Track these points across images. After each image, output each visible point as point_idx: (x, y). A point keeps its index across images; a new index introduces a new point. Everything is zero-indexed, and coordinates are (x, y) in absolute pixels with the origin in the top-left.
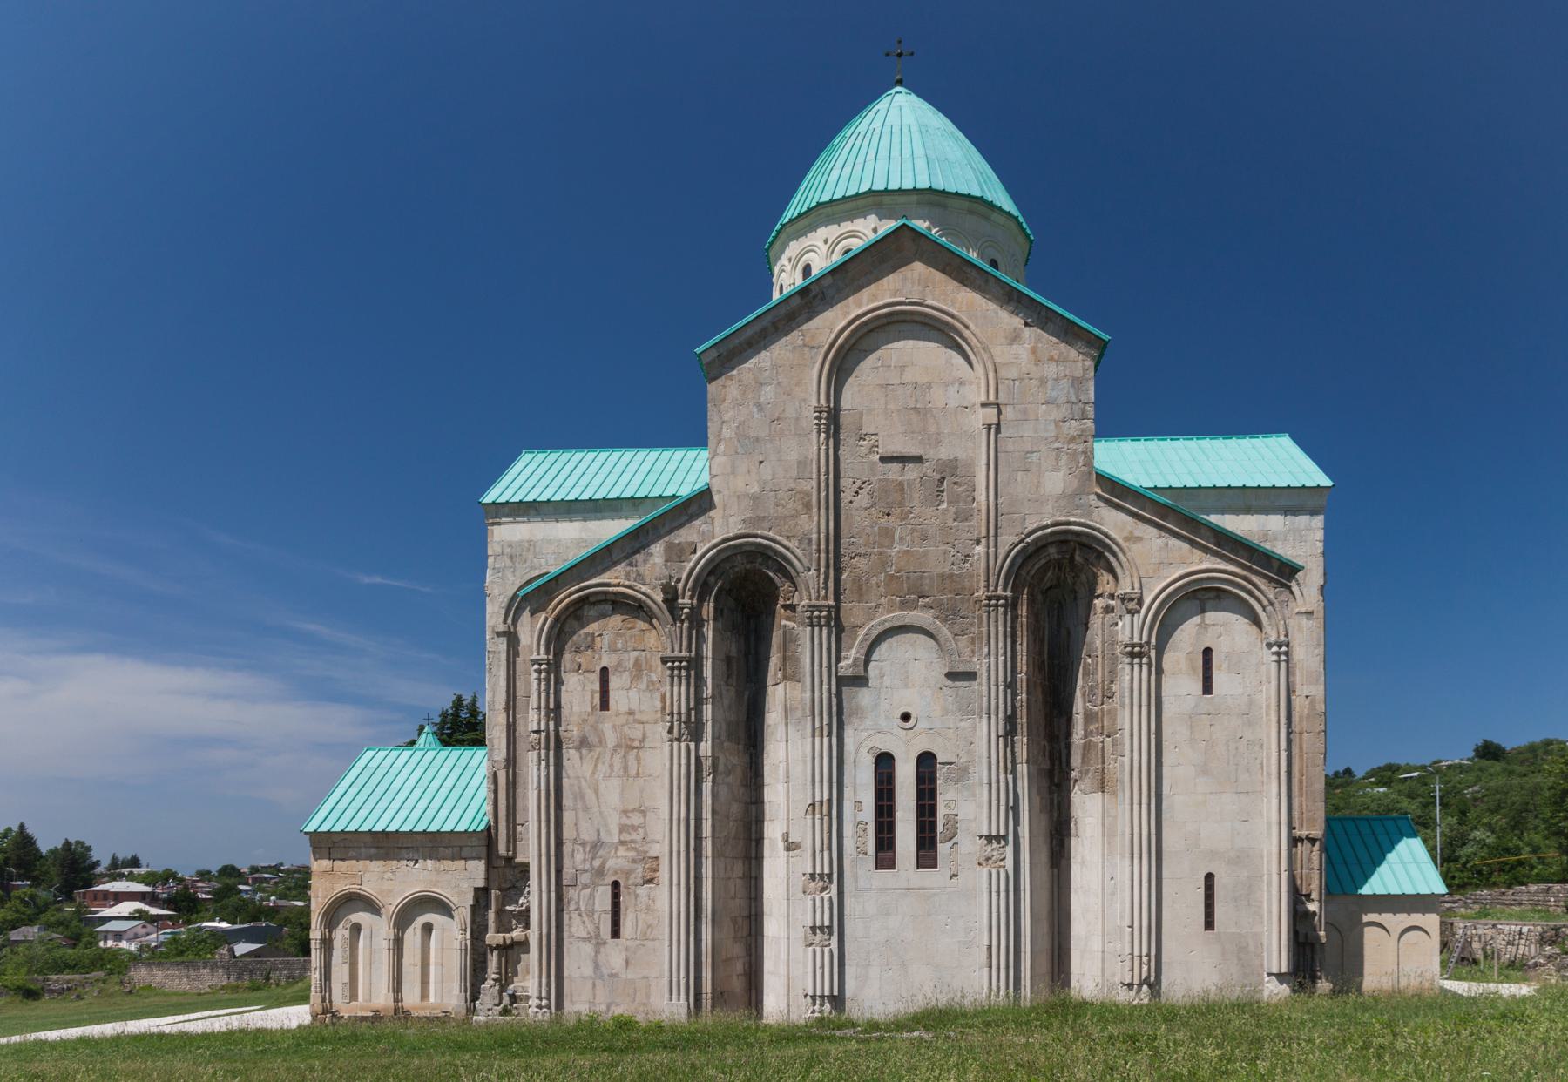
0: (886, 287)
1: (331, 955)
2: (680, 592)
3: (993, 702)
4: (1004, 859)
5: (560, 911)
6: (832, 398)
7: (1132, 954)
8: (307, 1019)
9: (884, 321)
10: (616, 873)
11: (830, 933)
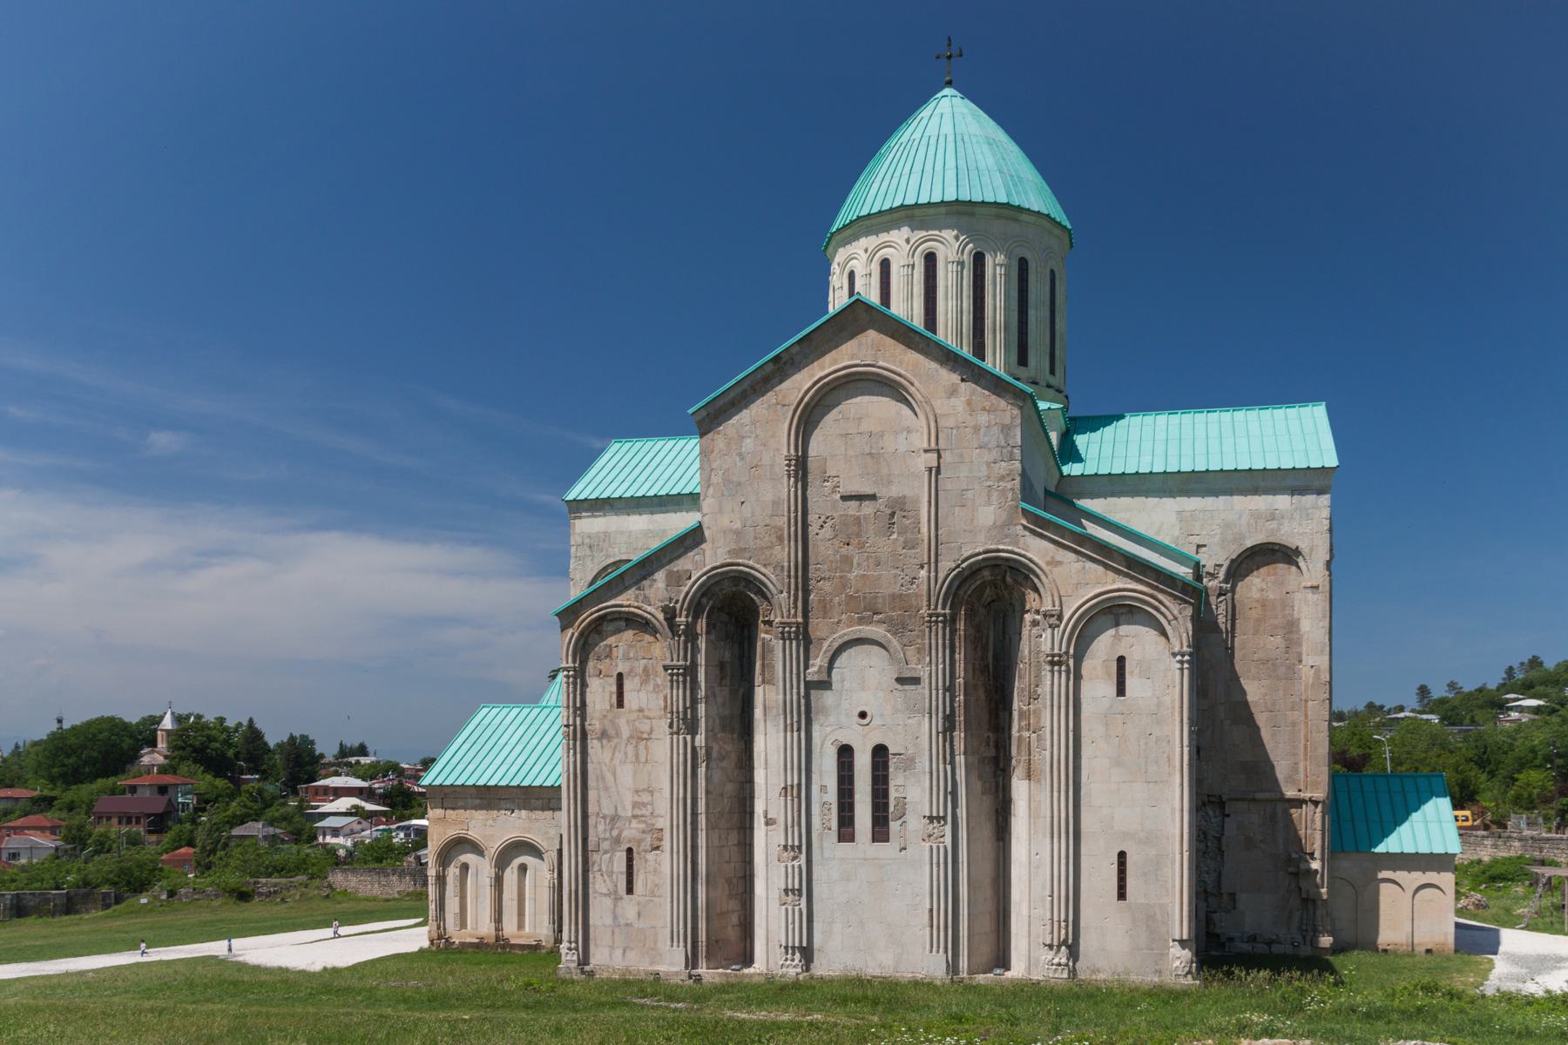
0: (844, 351)
1: (444, 890)
2: (678, 612)
3: (934, 703)
4: (944, 836)
5: (586, 871)
7: (1052, 919)
8: (426, 944)
9: (844, 380)
11: (800, 895)
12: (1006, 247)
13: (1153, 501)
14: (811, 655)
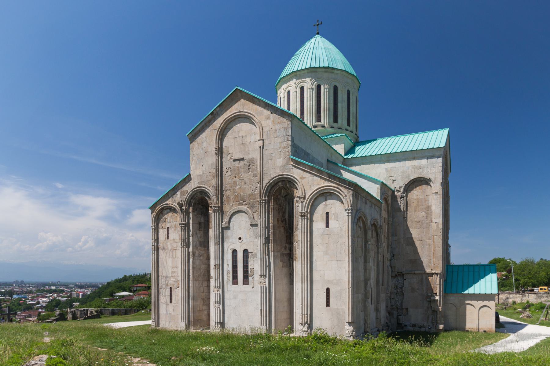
3: (262, 233)
4: (265, 282)
6: (220, 144)
7: (302, 314)
9: (233, 118)
10: (171, 285)
11: (220, 304)
12: (329, 82)
13: (377, 165)
14: (224, 217)
